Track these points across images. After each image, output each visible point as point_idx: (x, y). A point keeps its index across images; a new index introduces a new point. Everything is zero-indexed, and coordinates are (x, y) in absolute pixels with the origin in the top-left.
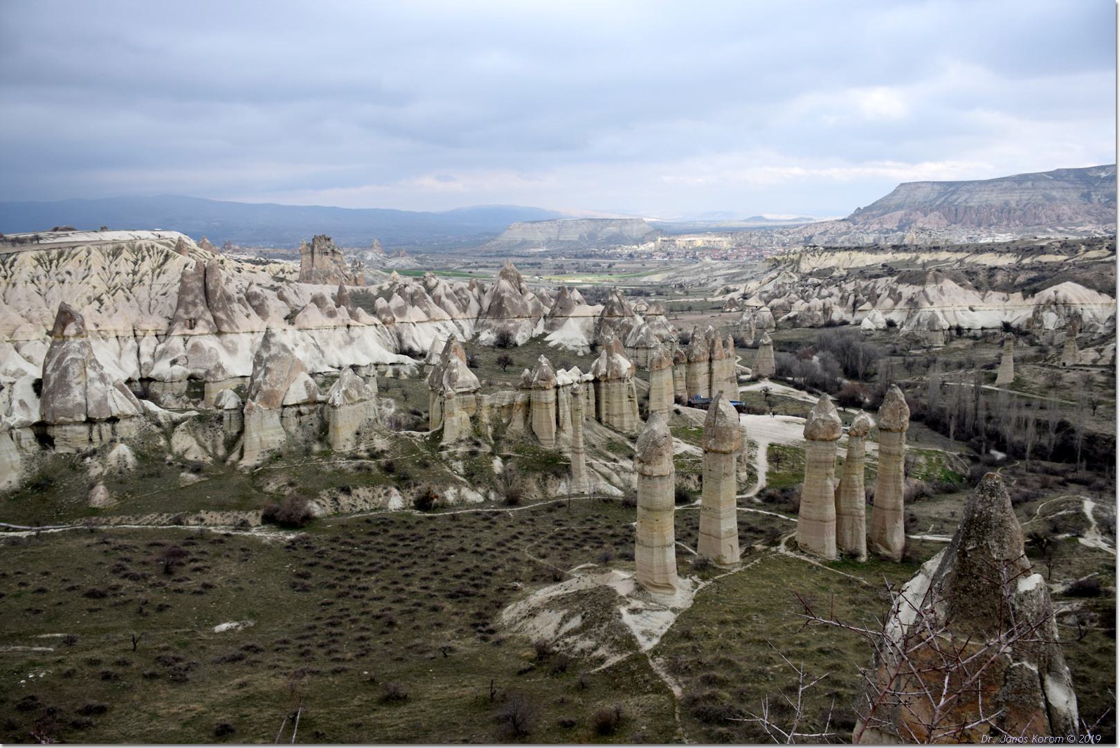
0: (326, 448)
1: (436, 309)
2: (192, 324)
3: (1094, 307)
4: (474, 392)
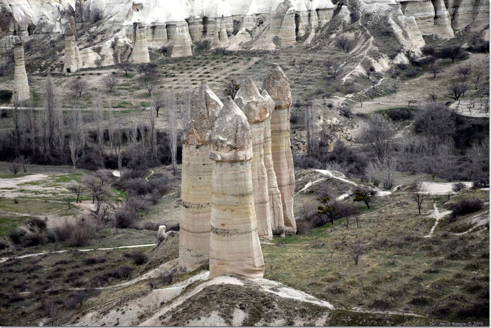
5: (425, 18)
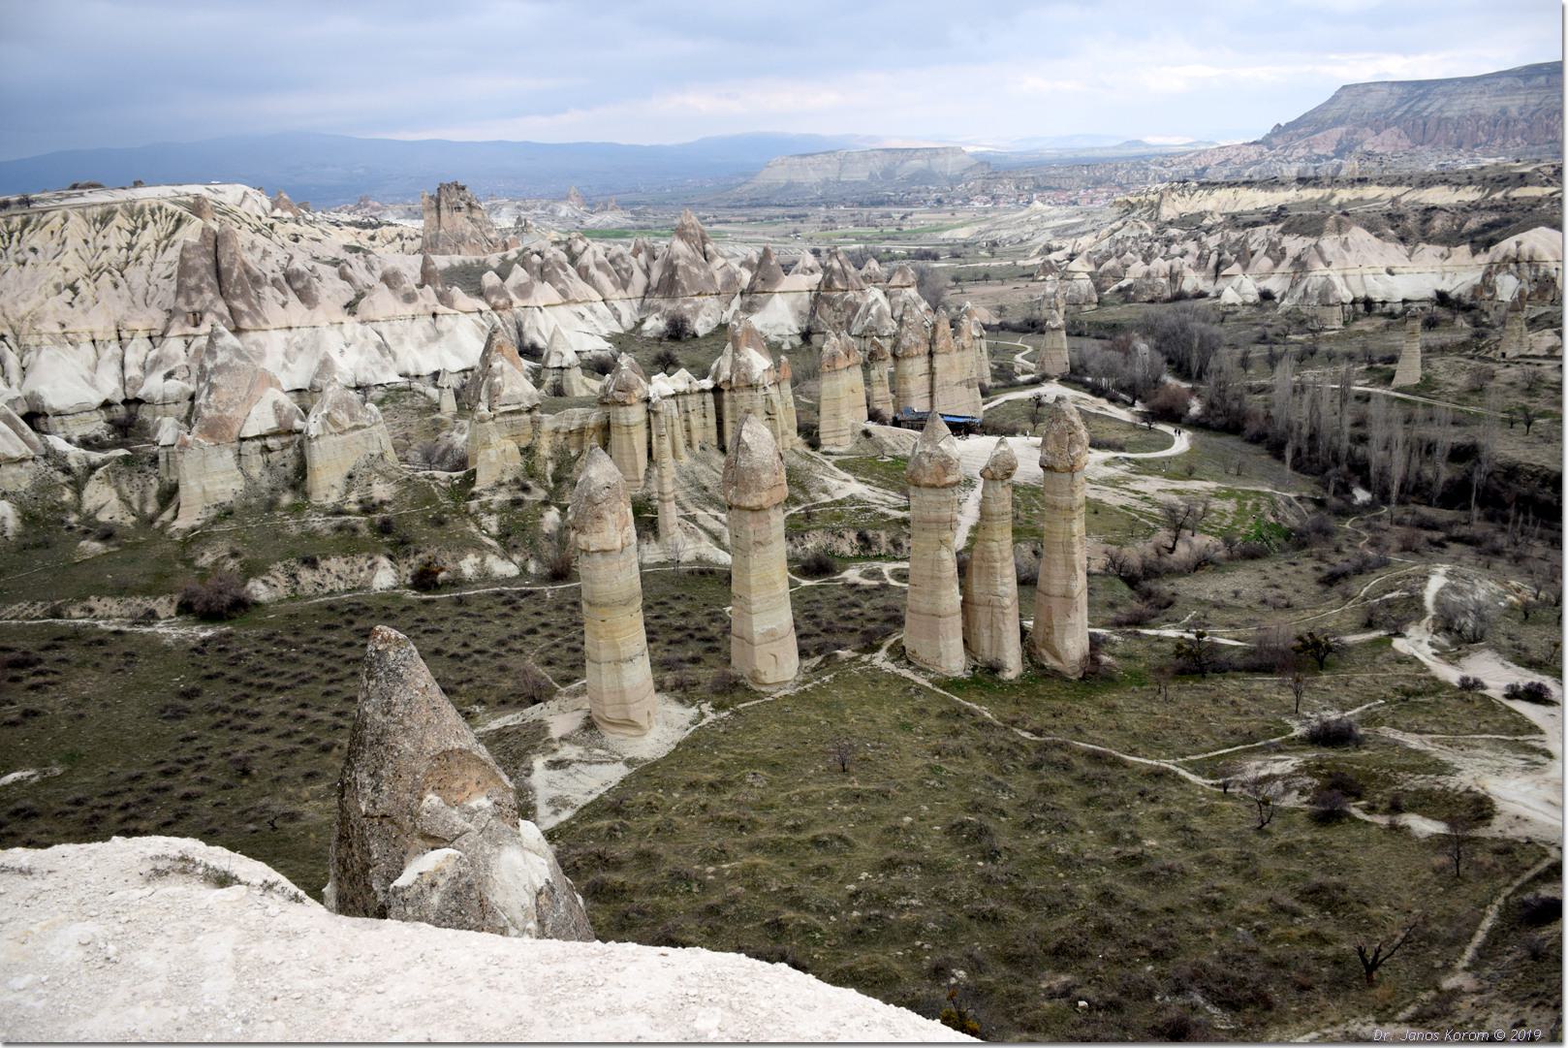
0: (300, 500)
1: (578, 287)
2: (197, 319)
4: (530, 411)
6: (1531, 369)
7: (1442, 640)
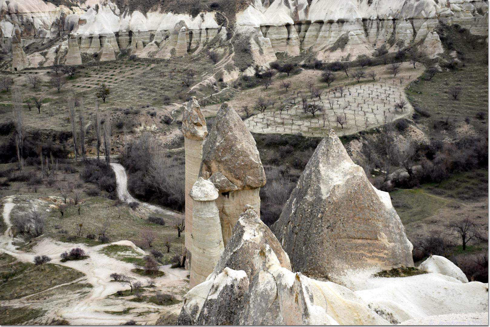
3: (43, 15)
5: (279, 40)
6: (33, 76)
7: (19, 240)
